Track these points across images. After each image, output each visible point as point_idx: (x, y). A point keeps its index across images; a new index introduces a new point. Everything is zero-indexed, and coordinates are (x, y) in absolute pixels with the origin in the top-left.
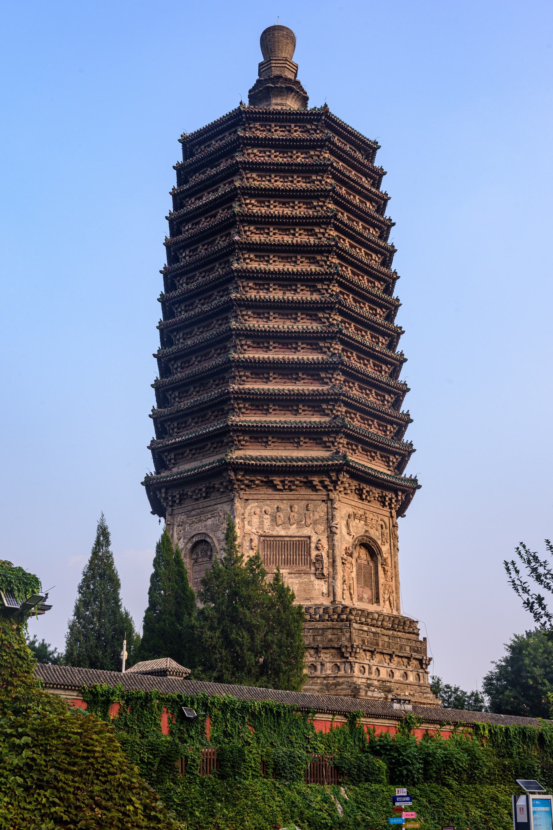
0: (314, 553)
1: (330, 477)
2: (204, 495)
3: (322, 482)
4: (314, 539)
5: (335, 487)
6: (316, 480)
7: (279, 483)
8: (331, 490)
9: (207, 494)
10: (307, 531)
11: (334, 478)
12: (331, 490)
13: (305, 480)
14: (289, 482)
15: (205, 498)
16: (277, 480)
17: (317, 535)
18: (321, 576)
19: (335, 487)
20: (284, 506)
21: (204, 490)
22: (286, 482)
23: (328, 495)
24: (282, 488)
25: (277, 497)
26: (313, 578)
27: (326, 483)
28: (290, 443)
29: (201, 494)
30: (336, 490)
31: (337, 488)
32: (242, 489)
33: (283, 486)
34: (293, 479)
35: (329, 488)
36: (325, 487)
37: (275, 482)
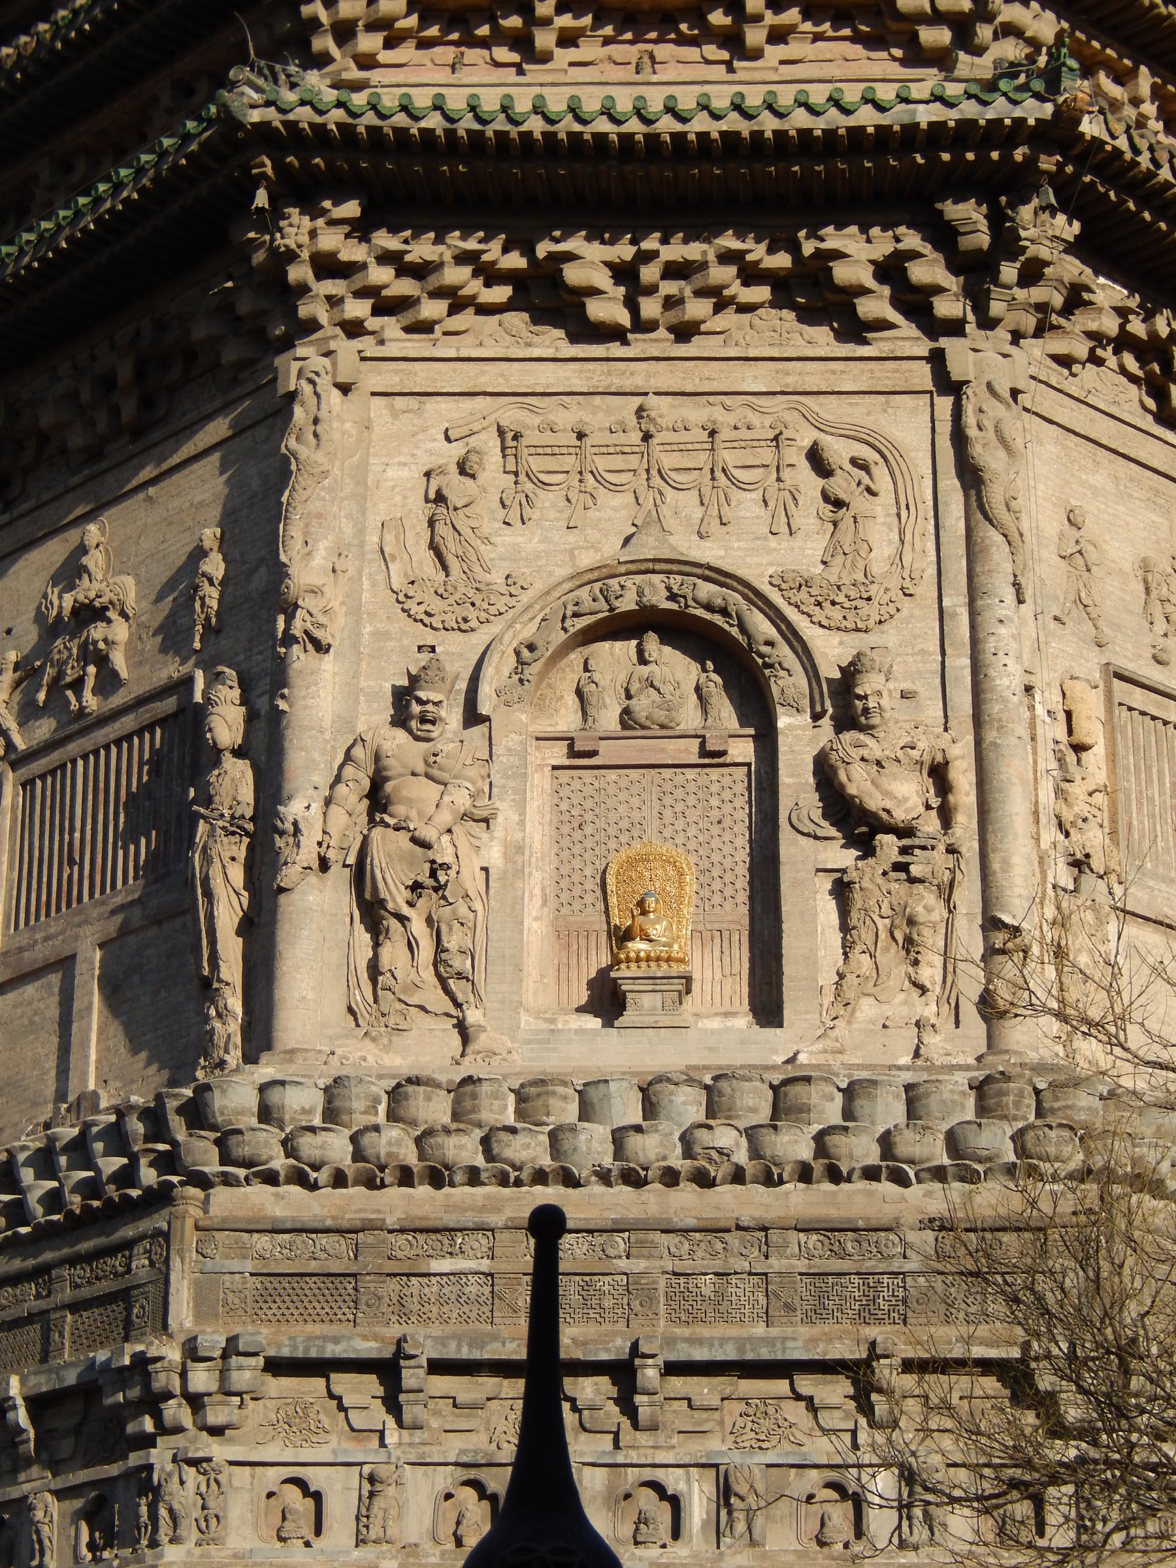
1: (944, 237)
2: (129, 410)
3: (890, 270)
6: (855, 253)
7: (602, 279)
8: (956, 328)
9: (147, 403)
13: (782, 260)
14: (674, 271)
15: (137, 432)
16: (589, 261)
21: (125, 372)
22: (649, 273)
23: (937, 359)
27: (919, 273)
28: (683, 41)
29: (115, 411)
30: (988, 323)
31: (996, 308)
32: (354, 329)
33: (631, 304)
34: (694, 251)
36: (915, 303)
37: (573, 274)
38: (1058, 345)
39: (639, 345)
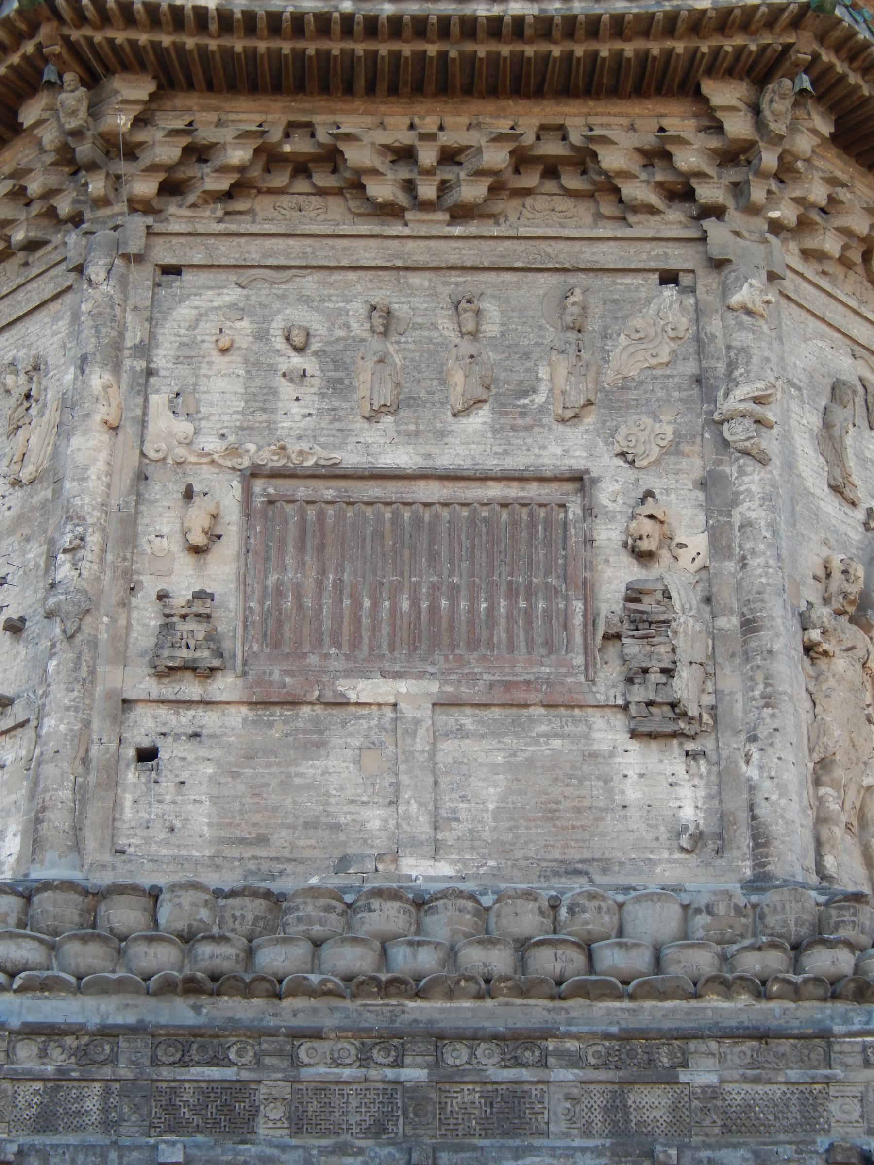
0: (616, 575)
4: (613, 489)
5: (738, 189)
10: (564, 448)
11: (738, 127)
12: (717, 212)
17: (632, 482)
18: (663, 723)
19: (738, 189)
20: (419, 302)
24: (402, 199)
25: (368, 253)
26: (608, 732)
27: (687, 159)
35: (707, 193)
36: (681, 193)
38: (811, 243)
39: (418, 222)
